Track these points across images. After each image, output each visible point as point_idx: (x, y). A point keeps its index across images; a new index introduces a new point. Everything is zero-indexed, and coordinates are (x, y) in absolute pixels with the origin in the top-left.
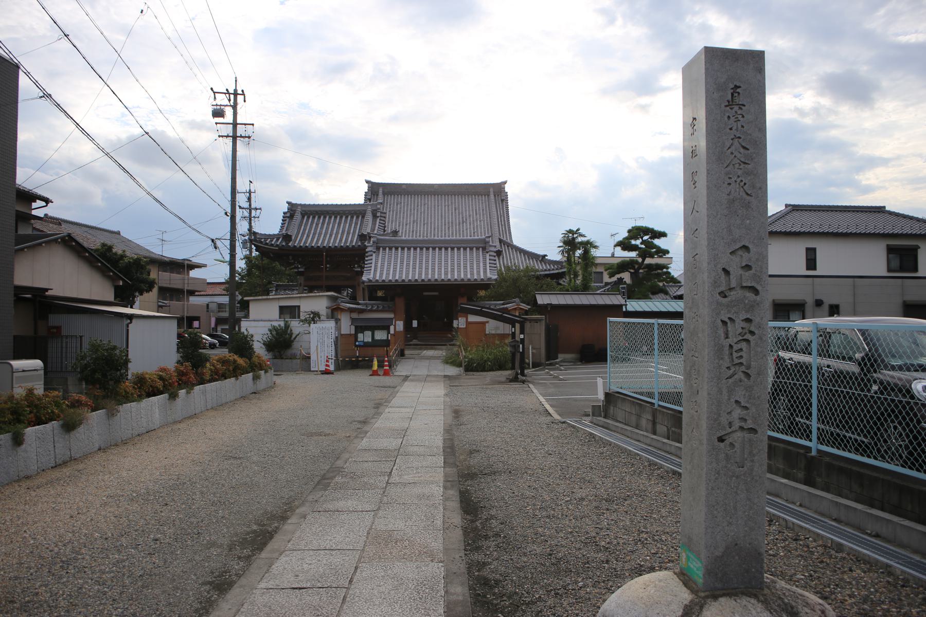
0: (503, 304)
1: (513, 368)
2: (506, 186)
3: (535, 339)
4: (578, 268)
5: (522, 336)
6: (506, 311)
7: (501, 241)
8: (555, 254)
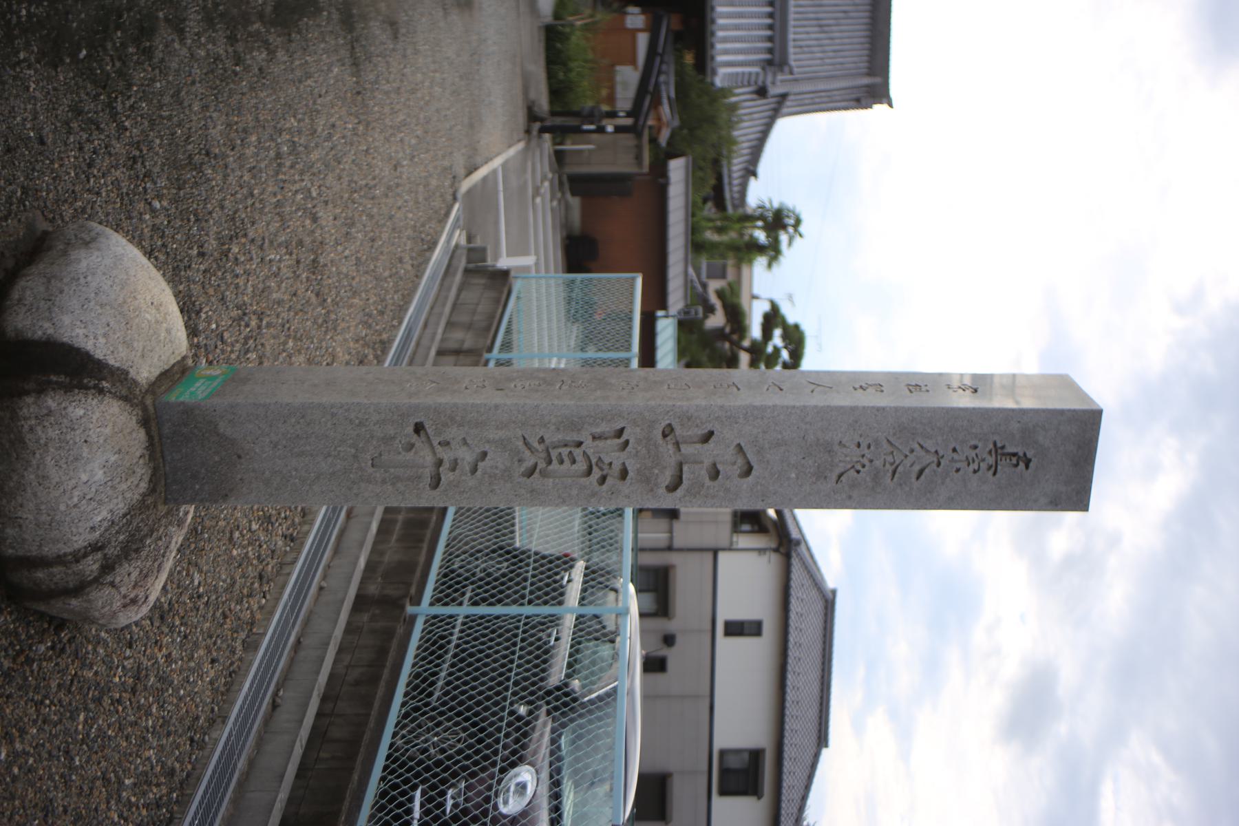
0: (669, 98)
1: (553, 114)
2: (885, 106)
3: (606, 153)
4: (733, 235)
5: (610, 129)
6: (656, 102)
7: (784, 97)
8: (759, 194)
